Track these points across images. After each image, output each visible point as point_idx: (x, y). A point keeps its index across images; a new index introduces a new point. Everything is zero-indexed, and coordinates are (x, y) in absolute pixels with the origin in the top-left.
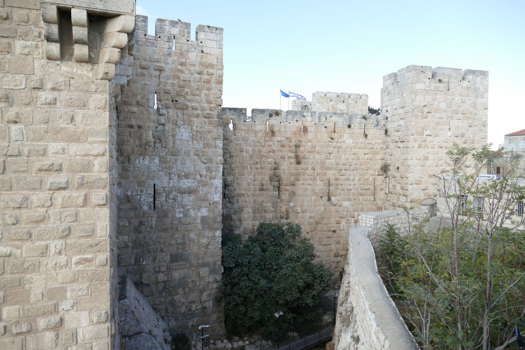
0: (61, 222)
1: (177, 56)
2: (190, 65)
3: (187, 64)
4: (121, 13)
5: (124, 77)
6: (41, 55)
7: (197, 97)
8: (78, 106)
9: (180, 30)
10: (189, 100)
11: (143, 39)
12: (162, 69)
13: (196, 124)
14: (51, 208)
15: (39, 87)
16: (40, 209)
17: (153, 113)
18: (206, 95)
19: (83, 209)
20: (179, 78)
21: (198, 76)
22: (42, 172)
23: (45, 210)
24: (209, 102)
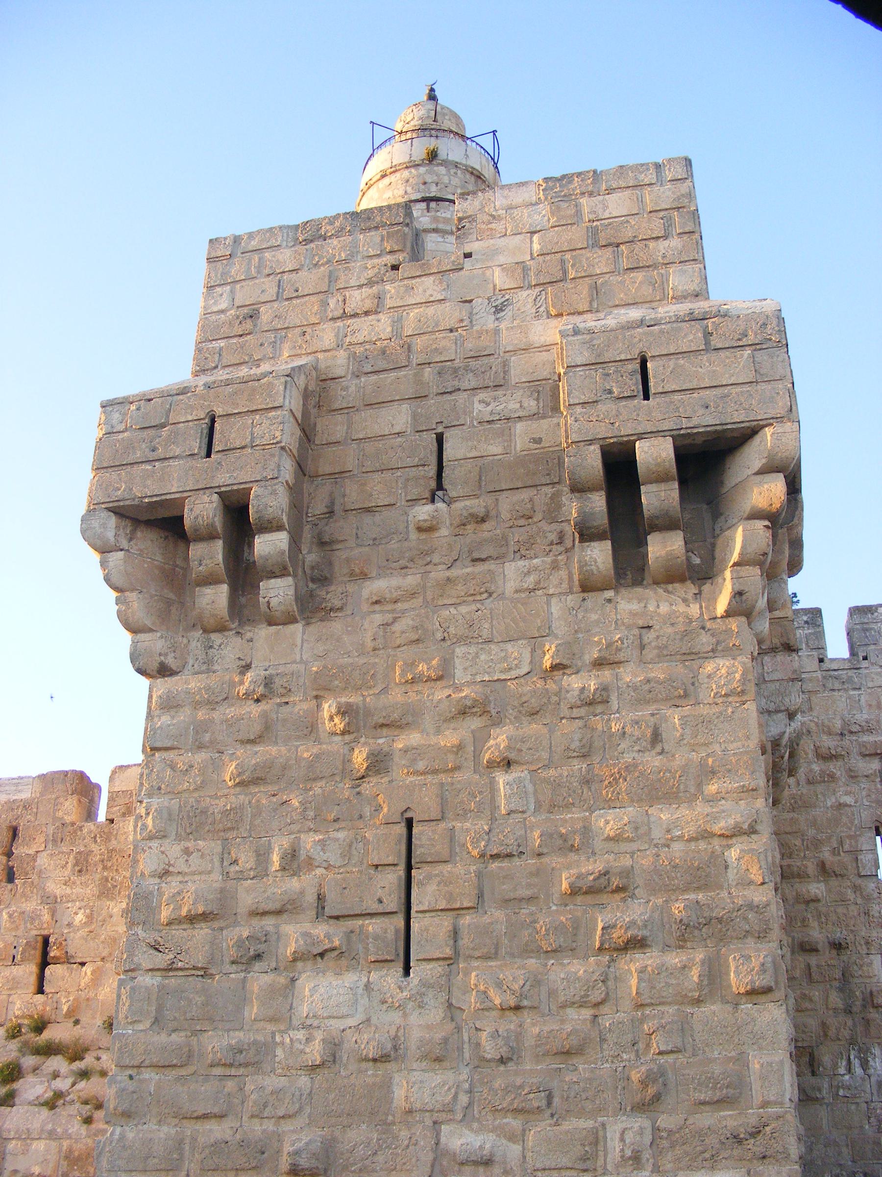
0: (637, 1055)
4: (761, 423)
6: (565, 585)
11: (814, 675)
14: (605, 1009)
15: (565, 662)
16: (571, 1013)
17: (876, 895)
19: (702, 1009)
22: (579, 899)
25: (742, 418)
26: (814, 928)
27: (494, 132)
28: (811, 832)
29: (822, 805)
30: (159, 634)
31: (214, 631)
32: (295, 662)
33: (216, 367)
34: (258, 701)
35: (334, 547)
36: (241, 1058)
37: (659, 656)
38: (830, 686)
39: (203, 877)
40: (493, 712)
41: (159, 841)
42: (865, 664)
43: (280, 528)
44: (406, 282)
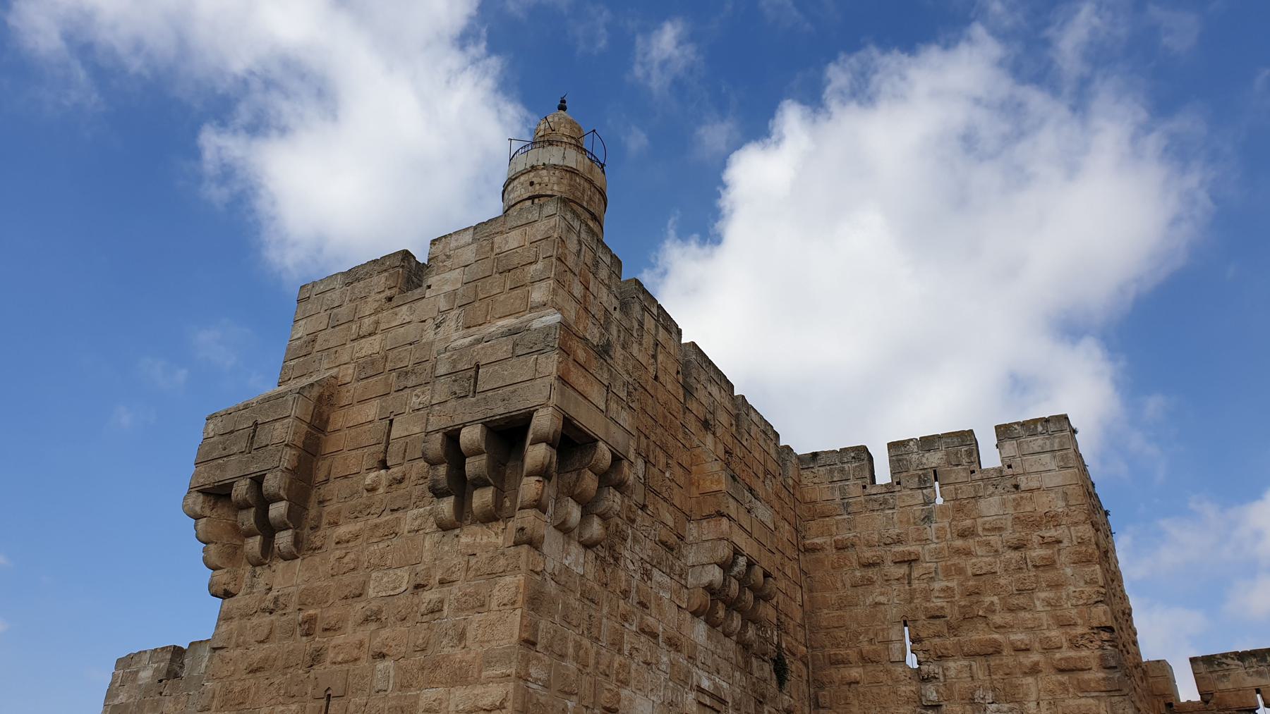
1: (947, 517)
2: (988, 530)
3: (980, 529)
4: (532, 409)
5: (710, 566)
7: (1022, 614)
8: (473, 608)
9: (947, 454)
10: (998, 627)
12: (913, 557)
13: (1034, 697)
15: (422, 583)
18: (1049, 604)
20: (960, 571)
21: (1016, 555)
24: (1065, 624)
26: (854, 705)
27: (594, 131)
28: (854, 626)
29: (862, 603)
30: (226, 570)
31: (257, 566)
32: (293, 585)
33: (289, 379)
34: (271, 613)
35: (325, 505)
37: (475, 576)
38: (871, 507)
40: (383, 619)
42: (898, 488)
43: (282, 499)
44: (394, 310)
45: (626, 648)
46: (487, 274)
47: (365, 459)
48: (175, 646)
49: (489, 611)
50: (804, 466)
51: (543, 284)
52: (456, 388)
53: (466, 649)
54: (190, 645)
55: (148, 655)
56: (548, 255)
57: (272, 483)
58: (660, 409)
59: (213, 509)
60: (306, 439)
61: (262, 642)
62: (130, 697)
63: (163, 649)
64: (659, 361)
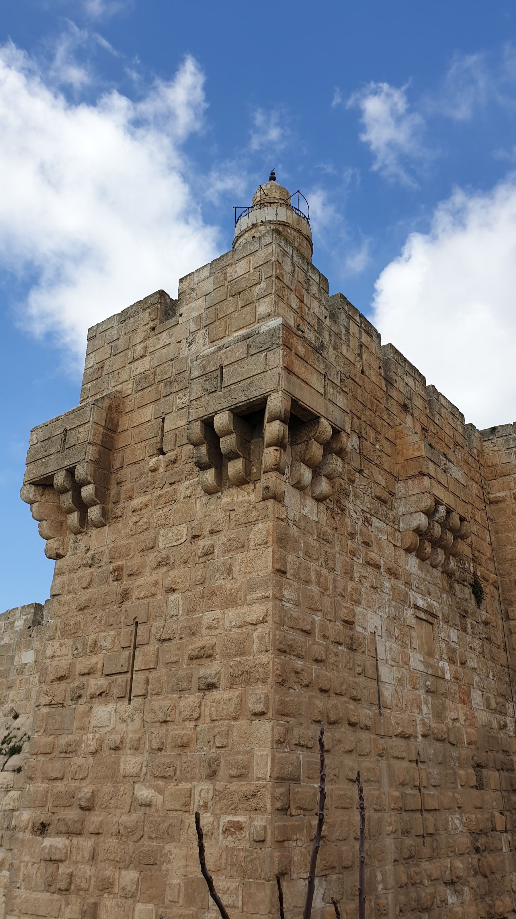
0: (210, 748)
4: (266, 395)
5: (417, 514)
8: (236, 549)
14: (200, 722)
15: (197, 534)
19: (237, 723)
23: (193, 726)
25: (243, 399)
27: (298, 191)
30: (56, 539)
31: (78, 534)
32: (104, 545)
34: (90, 567)
36: (70, 749)
37: (235, 525)
39: (65, 657)
40: (171, 563)
41: (53, 641)
43: (90, 483)
44: (157, 336)
45: (356, 576)
46: (223, 298)
47: (147, 449)
48: (36, 604)
49: (248, 550)
50: (485, 439)
51: (267, 299)
52: (207, 386)
53: (233, 580)
54: (46, 602)
55: (19, 611)
56: (269, 275)
57: (81, 472)
58: (368, 396)
59: (42, 495)
60: (103, 438)
61: (86, 588)
62: (11, 639)
63: (28, 606)
64: (364, 359)
